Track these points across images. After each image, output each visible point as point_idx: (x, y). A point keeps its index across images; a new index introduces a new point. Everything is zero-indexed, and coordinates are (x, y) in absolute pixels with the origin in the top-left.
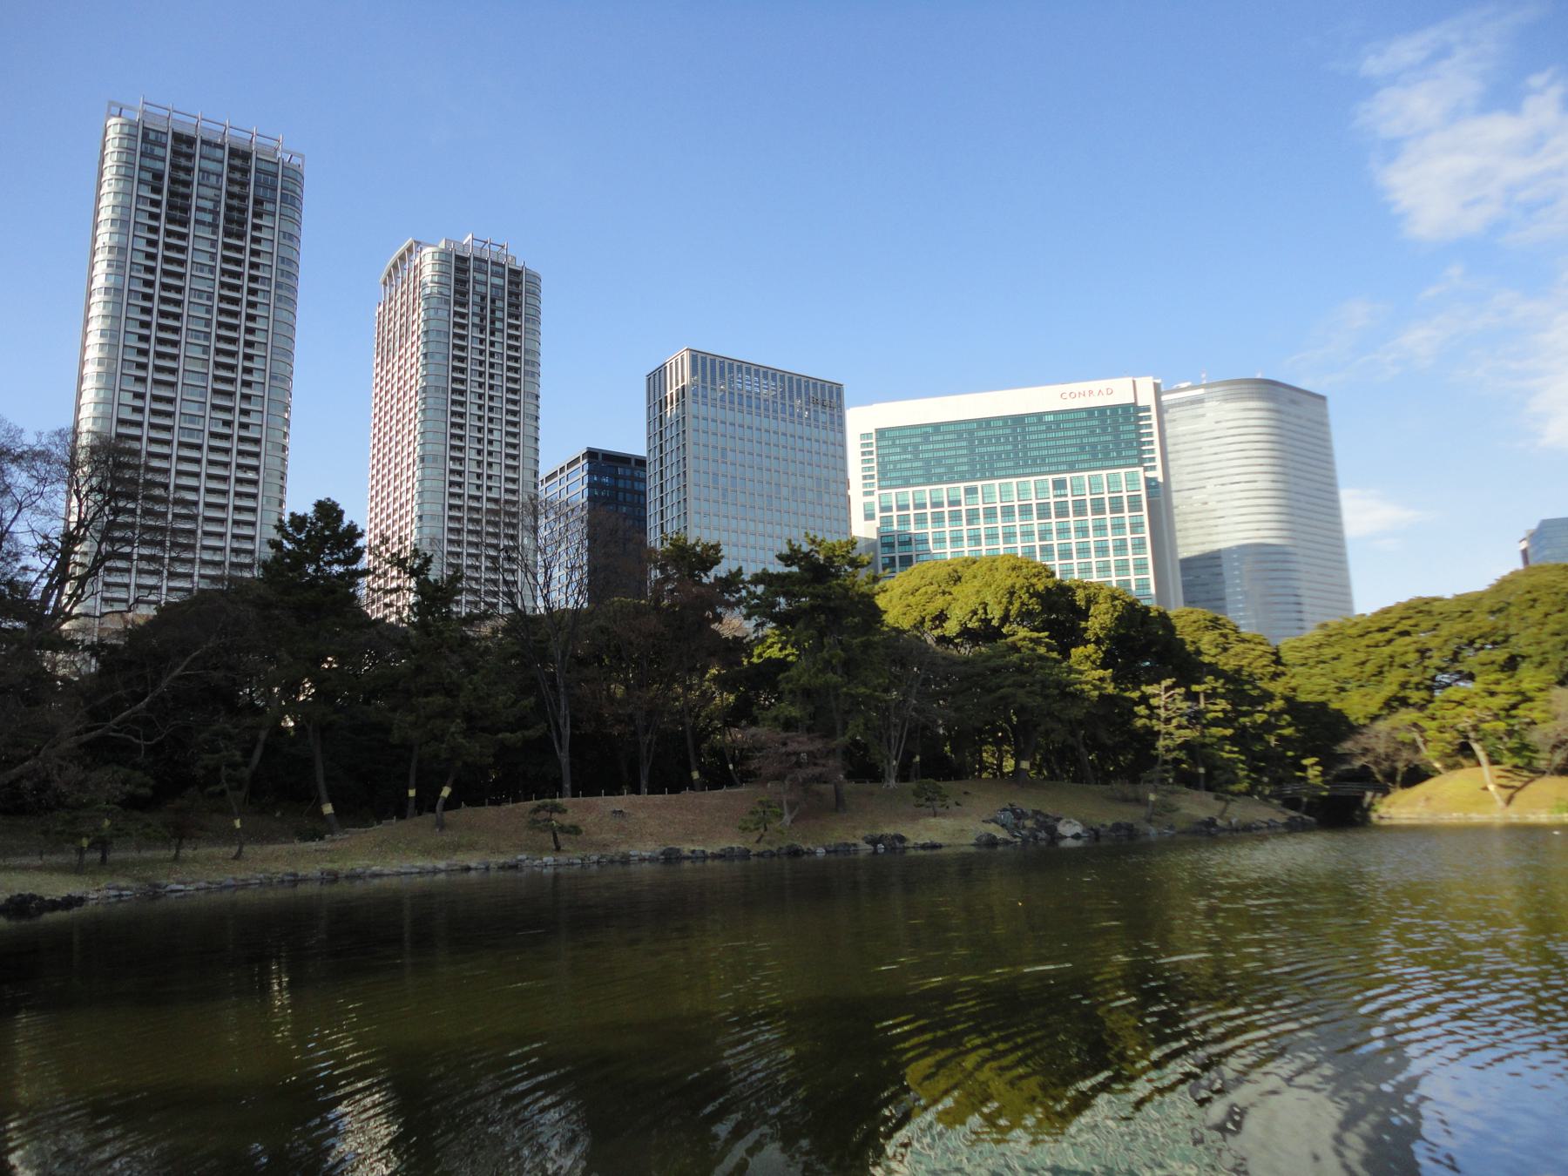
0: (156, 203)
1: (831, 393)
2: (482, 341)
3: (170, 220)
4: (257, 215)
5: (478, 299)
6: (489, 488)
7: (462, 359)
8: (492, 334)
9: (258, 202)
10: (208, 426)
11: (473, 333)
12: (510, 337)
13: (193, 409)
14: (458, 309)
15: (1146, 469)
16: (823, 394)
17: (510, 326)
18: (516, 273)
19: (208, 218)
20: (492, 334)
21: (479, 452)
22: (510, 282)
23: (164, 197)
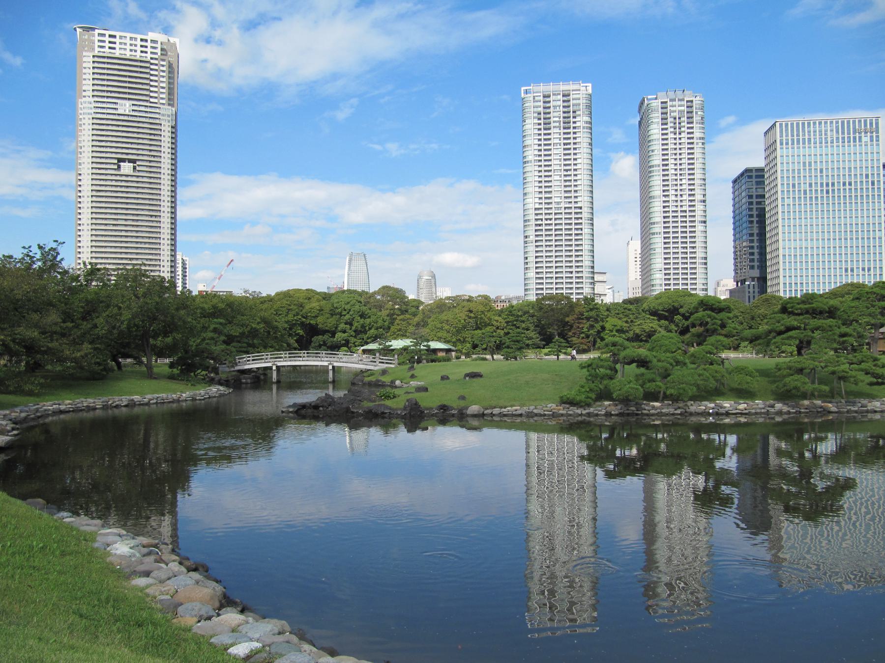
0: (540, 124)
2: (675, 139)
3: (545, 129)
4: (574, 117)
5: (672, 120)
9: (574, 112)
10: (563, 205)
13: (558, 200)
16: (865, 125)
19: (557, 124)
23: (542, 121)
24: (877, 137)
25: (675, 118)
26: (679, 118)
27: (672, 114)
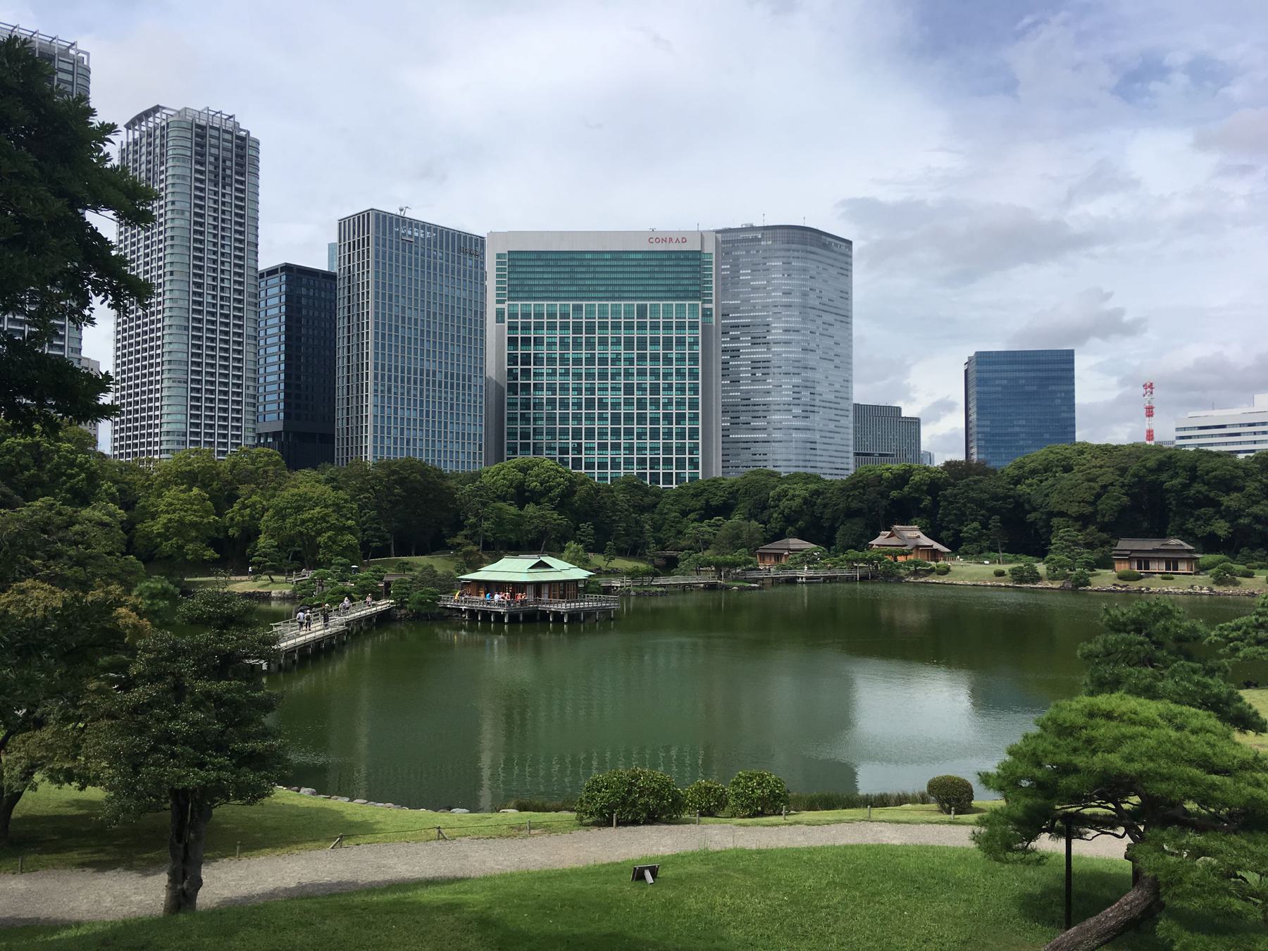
1: (476, 245)
2: (216, 193)
5: (212, 159)
6: (222, 307)
7: (201, 207)
8: (224, 187)
11: (209, 186)
12: (237, 189)
14: (198, 167)
15: (704, 302)
17: (237, 181)
18: (243, 139)
20: (224, 187)
21: (214, 279)
22: (237, 146)
24: (483, 263)
25: (217, 159)
26: (224, 161)
27: (214, 151)
